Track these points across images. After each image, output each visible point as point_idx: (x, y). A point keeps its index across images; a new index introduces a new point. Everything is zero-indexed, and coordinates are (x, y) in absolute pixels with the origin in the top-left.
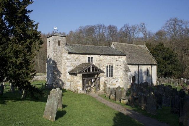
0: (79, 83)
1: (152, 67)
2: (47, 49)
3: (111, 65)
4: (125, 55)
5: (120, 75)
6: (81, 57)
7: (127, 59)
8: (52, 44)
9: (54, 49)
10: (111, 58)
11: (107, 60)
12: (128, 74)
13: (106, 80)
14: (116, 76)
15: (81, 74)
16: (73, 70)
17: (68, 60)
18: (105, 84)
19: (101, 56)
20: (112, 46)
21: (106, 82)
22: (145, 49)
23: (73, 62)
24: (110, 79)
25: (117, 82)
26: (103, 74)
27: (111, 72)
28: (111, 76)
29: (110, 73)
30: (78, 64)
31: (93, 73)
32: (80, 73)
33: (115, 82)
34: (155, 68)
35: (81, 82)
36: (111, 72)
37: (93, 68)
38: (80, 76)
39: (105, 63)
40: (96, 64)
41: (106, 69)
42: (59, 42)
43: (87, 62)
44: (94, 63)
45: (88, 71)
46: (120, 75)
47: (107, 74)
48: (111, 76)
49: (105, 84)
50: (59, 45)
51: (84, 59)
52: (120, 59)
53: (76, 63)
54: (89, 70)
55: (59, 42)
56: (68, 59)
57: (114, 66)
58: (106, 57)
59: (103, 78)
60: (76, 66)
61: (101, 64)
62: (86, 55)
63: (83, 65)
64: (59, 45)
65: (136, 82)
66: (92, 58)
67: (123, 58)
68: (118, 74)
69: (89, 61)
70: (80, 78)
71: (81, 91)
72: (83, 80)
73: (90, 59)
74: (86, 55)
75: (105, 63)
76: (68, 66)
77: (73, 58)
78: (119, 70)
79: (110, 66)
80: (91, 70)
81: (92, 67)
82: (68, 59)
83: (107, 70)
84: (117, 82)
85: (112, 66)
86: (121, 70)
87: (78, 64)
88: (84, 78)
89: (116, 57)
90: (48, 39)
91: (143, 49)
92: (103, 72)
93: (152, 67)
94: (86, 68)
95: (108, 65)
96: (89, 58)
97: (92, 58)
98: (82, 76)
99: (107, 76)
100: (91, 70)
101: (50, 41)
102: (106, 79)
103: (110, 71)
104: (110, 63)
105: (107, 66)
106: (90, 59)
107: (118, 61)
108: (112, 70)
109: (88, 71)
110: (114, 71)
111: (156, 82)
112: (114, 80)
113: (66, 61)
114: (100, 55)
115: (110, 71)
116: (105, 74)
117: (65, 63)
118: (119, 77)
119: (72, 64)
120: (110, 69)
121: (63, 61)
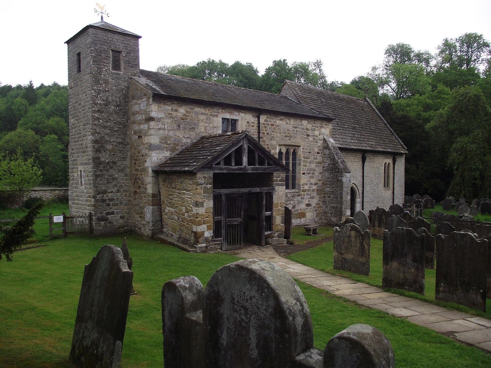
0: (201, 210)
4: (329, 120)
5: (316, 184)
6: (197, 114)
9: (97, 81)
10: (290, 127)
14: (306, 187)
15: (210, 174)
18: (288, 215)
19: (263, 118)
23: (171, 133)
24: (289, 195)
28: (290, 186)
30: (186, 138)
31: (250, 169)
32: (207, 166)
34: (401, 165)
35: (209, 204)
37: (251, 153)
38: (204, 178)
39: (274, 142)
45: (233, 164)
46: (316, 184)
48: (290, 186)
50: (116, 66)
52: (317, 133)
54: (239, 162)
55: (117, 53)
57: (300, 153)
60: (180, 148)
62: (215, 110)
63: (203, 142)
64: (116, 66)
71: (206, 240)
72: (217, 199)
74: (215, 110)
75: (274, 142)
77: (170, 116)
78: (313, 166)
79: (287, 153)
80: (245, 159)
81: (246, 146)
84: (308, 205)
85: (294, 153)
86: (319, 169)
87: (189, 141)
88: (218, 191)
89: (305, 122)
94: (227, 150)
95: (284, 150)
98: (211, 181)
100: (245, 159)
101: (79, 54)
104: (289, 142)
107: (311, 139)
108: (294, 165)
109: (233, 164)
112: (299, 198)
113: (142, 126)
114: (258, 112)
117: (140, 137)
118: (313, 190)
119: (164, 139)
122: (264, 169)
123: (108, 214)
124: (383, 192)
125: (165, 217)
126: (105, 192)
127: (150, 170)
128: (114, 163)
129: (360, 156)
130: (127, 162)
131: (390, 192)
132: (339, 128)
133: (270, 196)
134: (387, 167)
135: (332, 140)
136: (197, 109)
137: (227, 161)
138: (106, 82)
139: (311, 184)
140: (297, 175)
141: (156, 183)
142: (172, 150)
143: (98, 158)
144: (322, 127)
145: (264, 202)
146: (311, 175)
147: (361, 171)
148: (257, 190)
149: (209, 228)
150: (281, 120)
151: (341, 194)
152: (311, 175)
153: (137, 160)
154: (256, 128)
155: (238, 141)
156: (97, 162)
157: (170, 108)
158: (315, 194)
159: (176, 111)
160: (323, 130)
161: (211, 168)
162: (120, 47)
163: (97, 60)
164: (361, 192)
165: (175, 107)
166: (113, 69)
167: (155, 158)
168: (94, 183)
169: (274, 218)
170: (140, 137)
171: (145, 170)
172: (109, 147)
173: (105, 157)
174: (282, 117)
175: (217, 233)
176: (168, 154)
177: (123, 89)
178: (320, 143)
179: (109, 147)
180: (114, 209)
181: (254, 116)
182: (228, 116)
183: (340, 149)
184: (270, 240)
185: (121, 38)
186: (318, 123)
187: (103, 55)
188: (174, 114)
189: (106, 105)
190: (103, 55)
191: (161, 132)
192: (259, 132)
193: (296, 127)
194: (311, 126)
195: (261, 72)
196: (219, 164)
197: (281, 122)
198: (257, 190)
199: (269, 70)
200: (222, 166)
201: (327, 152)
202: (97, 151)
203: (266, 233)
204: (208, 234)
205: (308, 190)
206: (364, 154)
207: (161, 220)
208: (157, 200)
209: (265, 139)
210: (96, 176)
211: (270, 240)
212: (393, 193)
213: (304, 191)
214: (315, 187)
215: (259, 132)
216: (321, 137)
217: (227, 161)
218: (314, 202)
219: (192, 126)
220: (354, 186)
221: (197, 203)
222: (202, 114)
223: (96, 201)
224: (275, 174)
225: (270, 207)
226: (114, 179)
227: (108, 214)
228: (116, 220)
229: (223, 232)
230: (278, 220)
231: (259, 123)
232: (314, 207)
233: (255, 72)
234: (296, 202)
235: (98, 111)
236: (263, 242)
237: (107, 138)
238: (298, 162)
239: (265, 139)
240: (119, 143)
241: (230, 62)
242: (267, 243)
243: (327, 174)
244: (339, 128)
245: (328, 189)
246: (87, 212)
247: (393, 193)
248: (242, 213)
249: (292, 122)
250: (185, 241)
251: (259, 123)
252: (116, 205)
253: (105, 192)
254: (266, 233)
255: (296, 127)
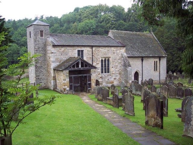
0: (65, 82)
1: (160, 61)
2: (28, 41)
3: (107, 59)
4: (124, 46)
5: (118, 71)
7: (127, 51)
8: (32, 35)
9: (35, 41)
10: (106, 51)
11: (102, 53)
12: (128, 69)
13: (101, 77)
14: (114, 72)
15: (68, 71)
16: (59, 66)
17: (52, 54)
19: (94, 49)
20: (110, 34)
21: (100, 80)
22: (152, 37)
23: (59, 57)
25: (115, 79)
26: (94, 70)
27: (107, 68)
28: (107, 72)
29: (105, 69)
30: (64, 58)
31: (82, 69)
32: (66, 69)
33: (112, 79)
35: (68, 80)
36: (107, 68)
40: (87, 58)
41: (100, 63)
42: (42, 32)
43: (76, 56)
44: (85, 59)
46: (118, 71)
47: (102, 69)
48: (107, 72)
49: (97, 83)
50: (42, 35)
51: (73, 53)
52: (118, 52)
53: (62, 57)
55: (42, 32)
56: (53, 53)
57: (111, 59)
58: (100, 49)
59: (95, 75)
60: (62, 62)
61: (93, 58)
62: (75, 48)
64: (42, 35)
65: (140, 79)
66: (82, 51)
67: (123, 51)
68: (117, 70)
69: (79, 55)
70: (66, 76)
71: (67, 90)
72: (70, 78)
73: (81, 53)
76: (53, 62)
78: (117, 64)
79: (105, 60)
80: (80, 66)
82: (53, 53)
83: (102, 64)
84: (115, 79)
85: (108, 60)
86: (120, 65)
87: (65, 59)
88: (71, 76)
89: (113, 48)
90: (28, 29)
91: (150, 38)
92: (95, 68)
93: (160, 61)
94: (73, 63)
95: (104, 59)
96: (79, 51)
97: (82, 51)
99: (102, 72)
100: (80, 66)
102: (100, 76)
103: (105, 66)
104: (106, 56)
105: (102, 60)
106: (81, 53)
107: (115, 54)
108: (108, 64)
110: (111, 66)
111: (166, 78)
112: (111, 76)
114: (92, 47)
115: (105, 66)
116: (100, 70)
117: (49, 58)
119: (57, 59)
120: (105, 64)
121: (48, 55)
122: (88, 68)
123: (40, 83)
124: (154, 73)
125: (57, 84)
126: (39, 76)
127: (52, 69)
128: (42, 66)
129: (140, 59)
130: (46, 66)
131: (158, 73)
132: (131, 48)
133: (90, 77)
134: (156, 63)
135: (125, 54)
136: (68, 48)
137: (74, 66)
138: (39, 41)
139: (116, 71)
140: (110, 68)
141: (54, 73)
142: (60, 62)
143: (36, 65)
144: (121, 49)
145: (88, 79)
146: (116, 68)
147: (142, 65)
148: (85, 75)
149: (68, 87)
150: (102, 48)
151: (127, 75)
152: (116, 68)
153: (48, 65)
154: (91, 52)
155: (77, 60)
156: (36, 67)
157: (58, 49)
158: (118, 75)
159: (61, 49)
160: (121, 50)
161: (68, 69)
162: (43, 29)
163: (35, 35)
164: (141, 73)
165: (60, 48)
166: (41, 36)
167: (53, 65)
168: (35, 73)
169: (92, 84)
170: (49, 58)
171: (51, 69)
172: (40, 62)
173: (38, 65)
174: (102, 47)
175: (71, 88)
176: (58, 64)
177: (44, 43)
178: (120, 55)
179: (40, 62)
180: (42, 81)
181: (90, 48)
182: (80, 49)
183: (128, 57)
184: (90, 91)
185: (43, 26)
186: (119, 48)
187: (37, 33)
188: (60, 50)
189: (39, 48)
190: (37, 33)
191: (56, 57)
192: (92, 54)
193: (108, 51)
194: (115, 49)
195: (126, 10)
196: (71, 67)
197: (102, 49)
198: (85, 75)
199: (129, 10)
200: (72, 68)
201: (122, 59)
202: (36, 63)
203: (89, 89)
204: (68, 89)
205: (114, 73)
206: (142, 58)
207: (56, 85)
208: (55, 79)
209: (95, 56)
210: (36, 71)
211: (90, 91)
212: (160, 73)
213: (113, 74)
214: (118, 72)
215: (92, 54)
216: (120, 53)
217: (74, 66)
218: (117, 78)
219: (67, 54)
220: (138, 71)
221: (63, 79)
222: (70, 49)
223: (36, 79)
224: (92, 70)
225: (90, 80)
226: (42, 72)
227: (40, 83)
228: (43, 85)
229: (73, 88)
230: (93, 84)
231: (92, 50)
232: (118, 80)
233: (123, 9)
234: (109, 78)
235: (36, 51)
236: (88, 92)
237: (39, 59)
238: (110, 63)
239: (95, 56)
240: (43, 60)
241: (110, 5)
242: (89, 92)
243: (122, 67)
244: (131, 48)
245: (123, 73)
246: (34, 82)
247: (160, 73)
248: (80, 82)
249: (107, 49)
250: (62, 91)
251: (92, 50)
252: (43, 80)
253: (39, 76)
254: (89, 89)
255: (108, 51)
